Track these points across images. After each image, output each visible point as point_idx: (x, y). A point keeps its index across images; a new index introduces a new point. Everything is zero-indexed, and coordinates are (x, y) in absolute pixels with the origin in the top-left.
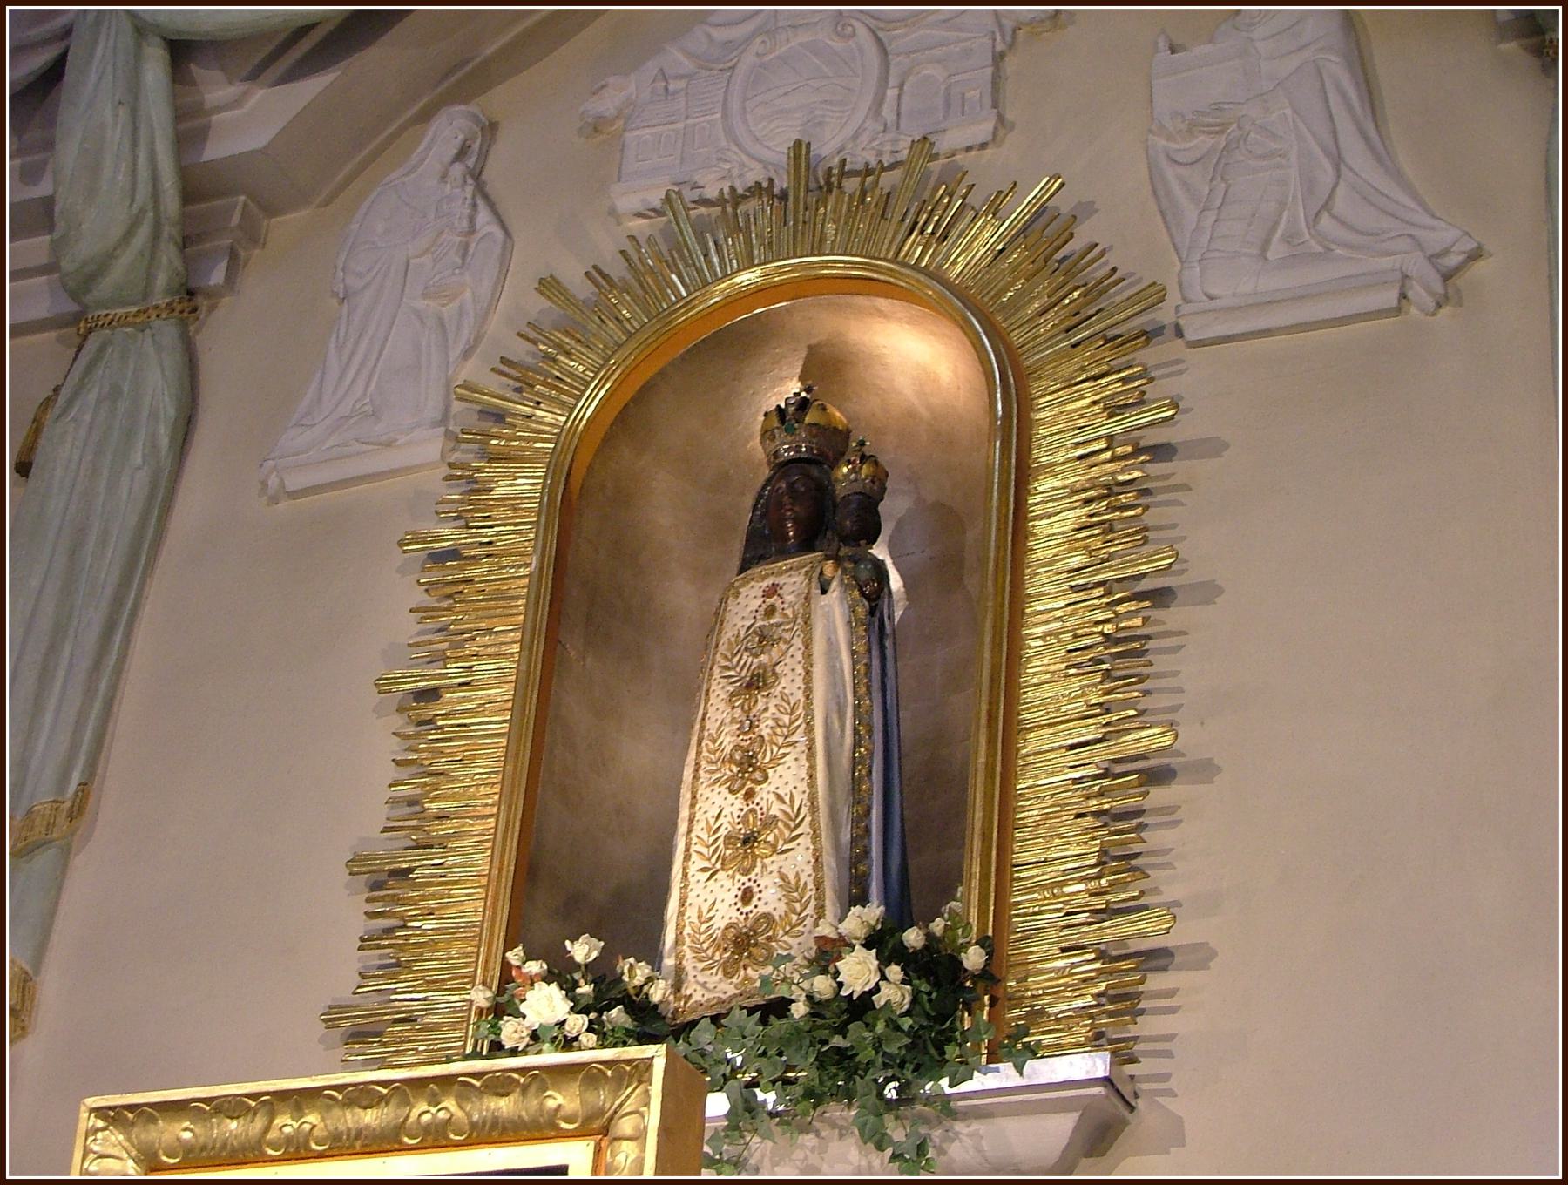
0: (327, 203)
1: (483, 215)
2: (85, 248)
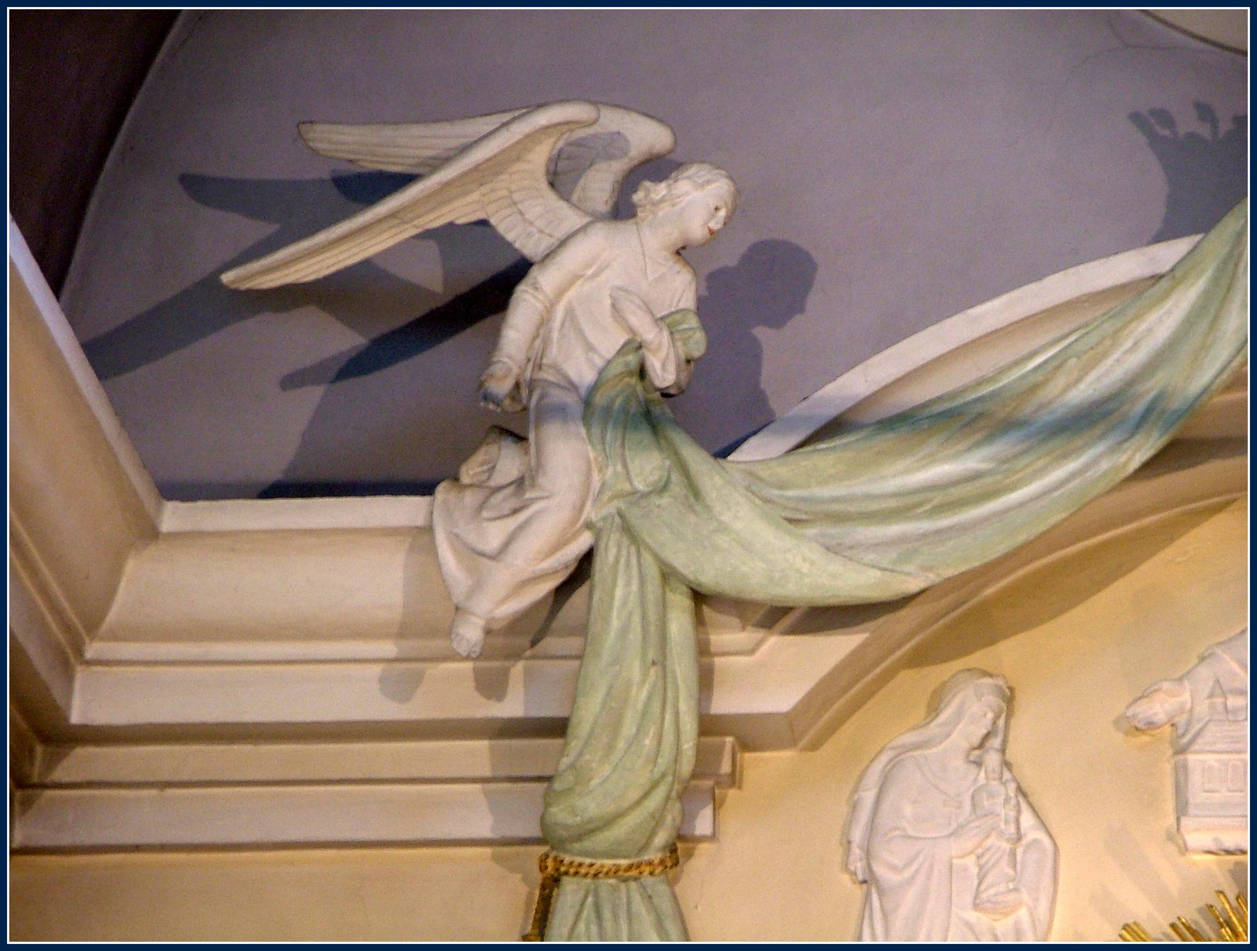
0: (815, 746)
1: (1027, 819)
2: (591, 805)
